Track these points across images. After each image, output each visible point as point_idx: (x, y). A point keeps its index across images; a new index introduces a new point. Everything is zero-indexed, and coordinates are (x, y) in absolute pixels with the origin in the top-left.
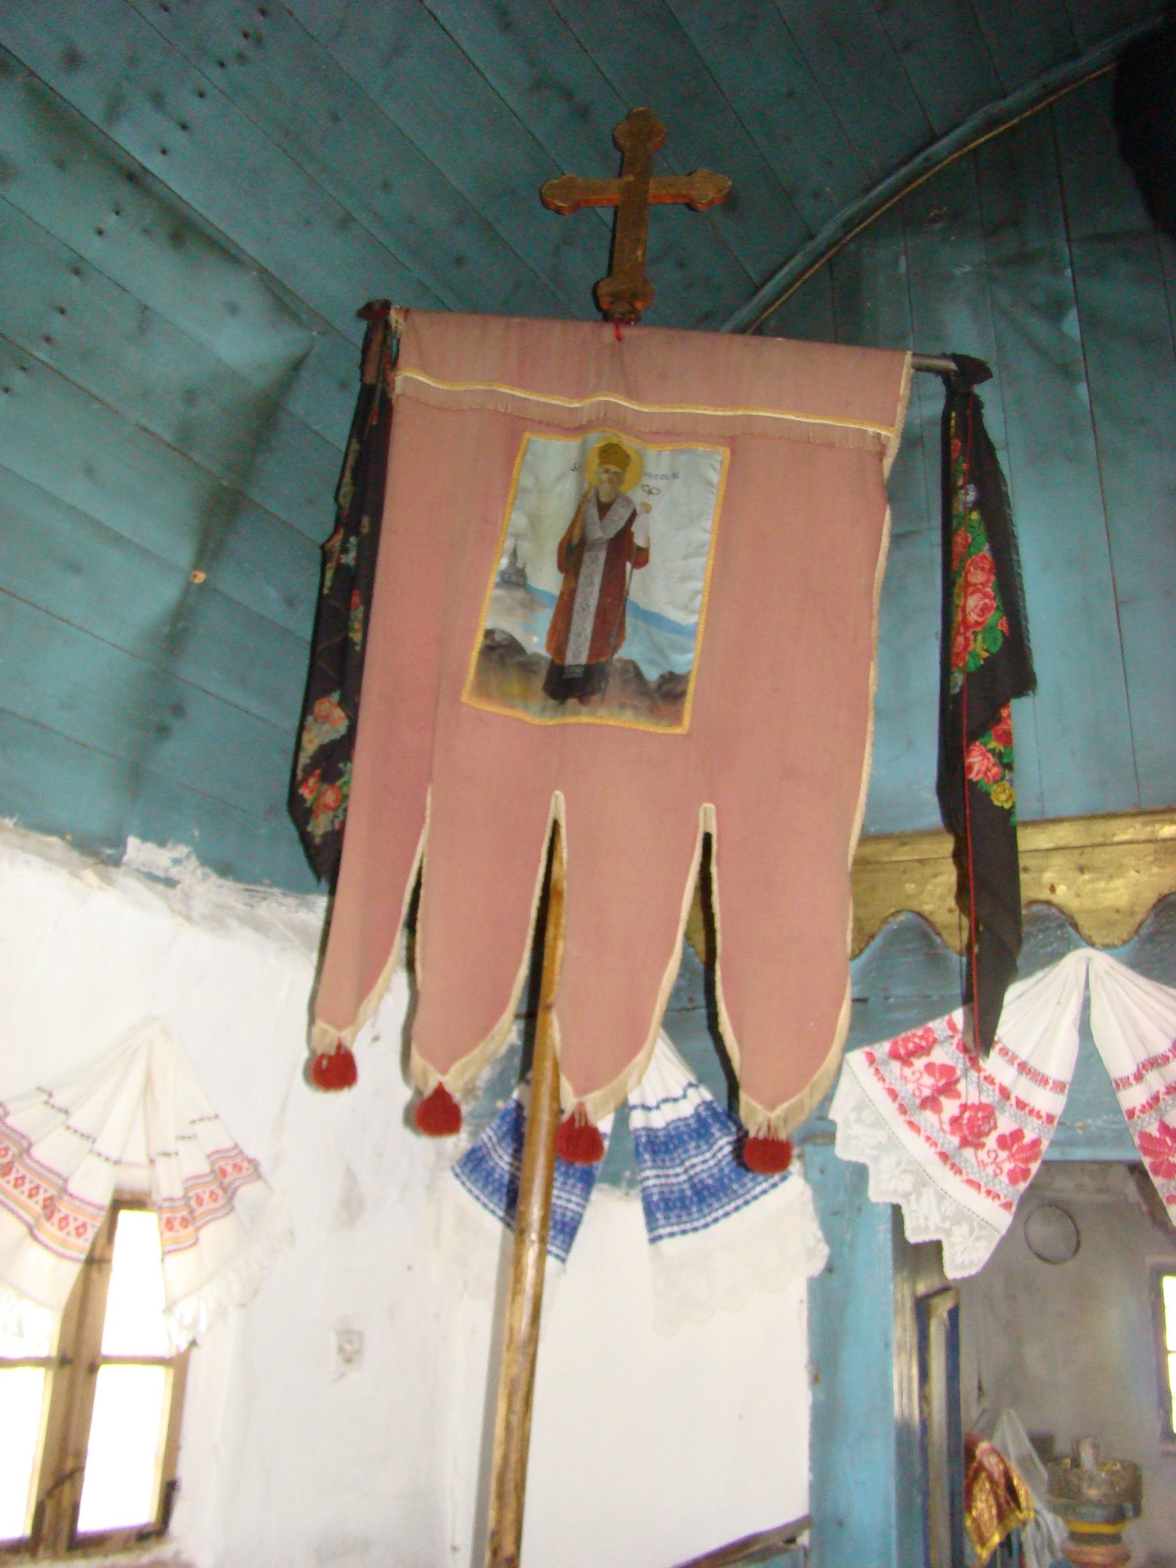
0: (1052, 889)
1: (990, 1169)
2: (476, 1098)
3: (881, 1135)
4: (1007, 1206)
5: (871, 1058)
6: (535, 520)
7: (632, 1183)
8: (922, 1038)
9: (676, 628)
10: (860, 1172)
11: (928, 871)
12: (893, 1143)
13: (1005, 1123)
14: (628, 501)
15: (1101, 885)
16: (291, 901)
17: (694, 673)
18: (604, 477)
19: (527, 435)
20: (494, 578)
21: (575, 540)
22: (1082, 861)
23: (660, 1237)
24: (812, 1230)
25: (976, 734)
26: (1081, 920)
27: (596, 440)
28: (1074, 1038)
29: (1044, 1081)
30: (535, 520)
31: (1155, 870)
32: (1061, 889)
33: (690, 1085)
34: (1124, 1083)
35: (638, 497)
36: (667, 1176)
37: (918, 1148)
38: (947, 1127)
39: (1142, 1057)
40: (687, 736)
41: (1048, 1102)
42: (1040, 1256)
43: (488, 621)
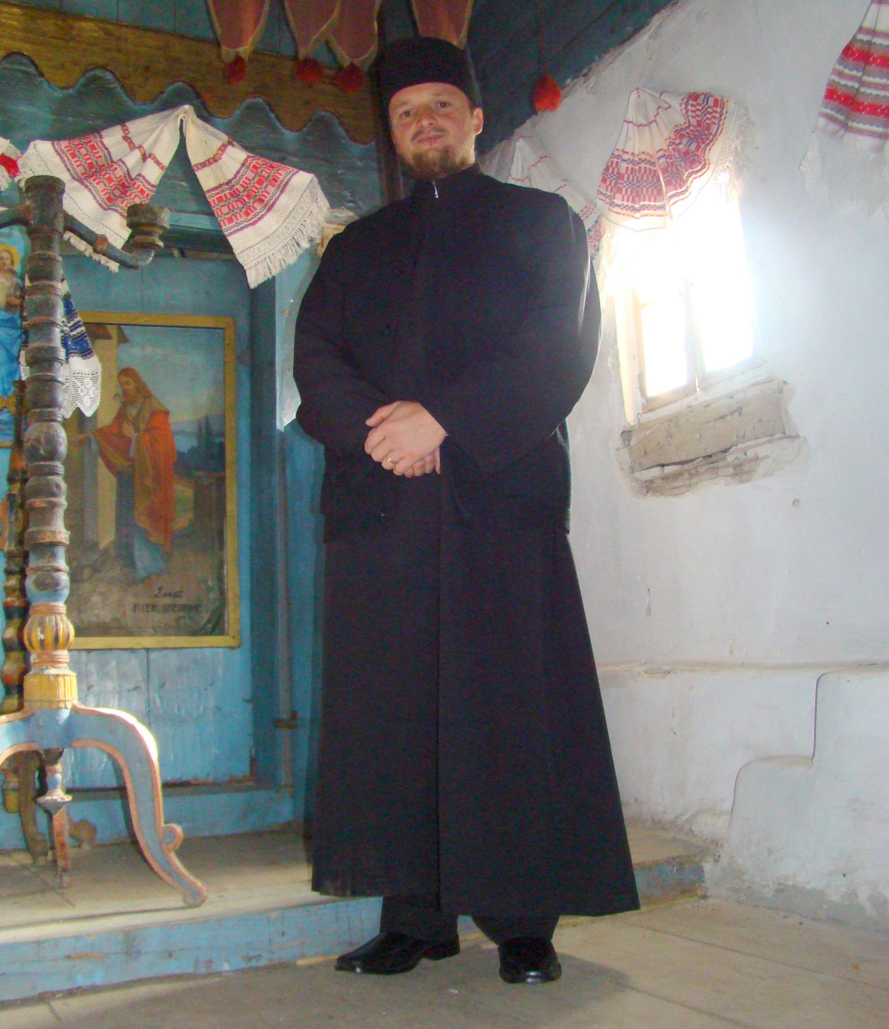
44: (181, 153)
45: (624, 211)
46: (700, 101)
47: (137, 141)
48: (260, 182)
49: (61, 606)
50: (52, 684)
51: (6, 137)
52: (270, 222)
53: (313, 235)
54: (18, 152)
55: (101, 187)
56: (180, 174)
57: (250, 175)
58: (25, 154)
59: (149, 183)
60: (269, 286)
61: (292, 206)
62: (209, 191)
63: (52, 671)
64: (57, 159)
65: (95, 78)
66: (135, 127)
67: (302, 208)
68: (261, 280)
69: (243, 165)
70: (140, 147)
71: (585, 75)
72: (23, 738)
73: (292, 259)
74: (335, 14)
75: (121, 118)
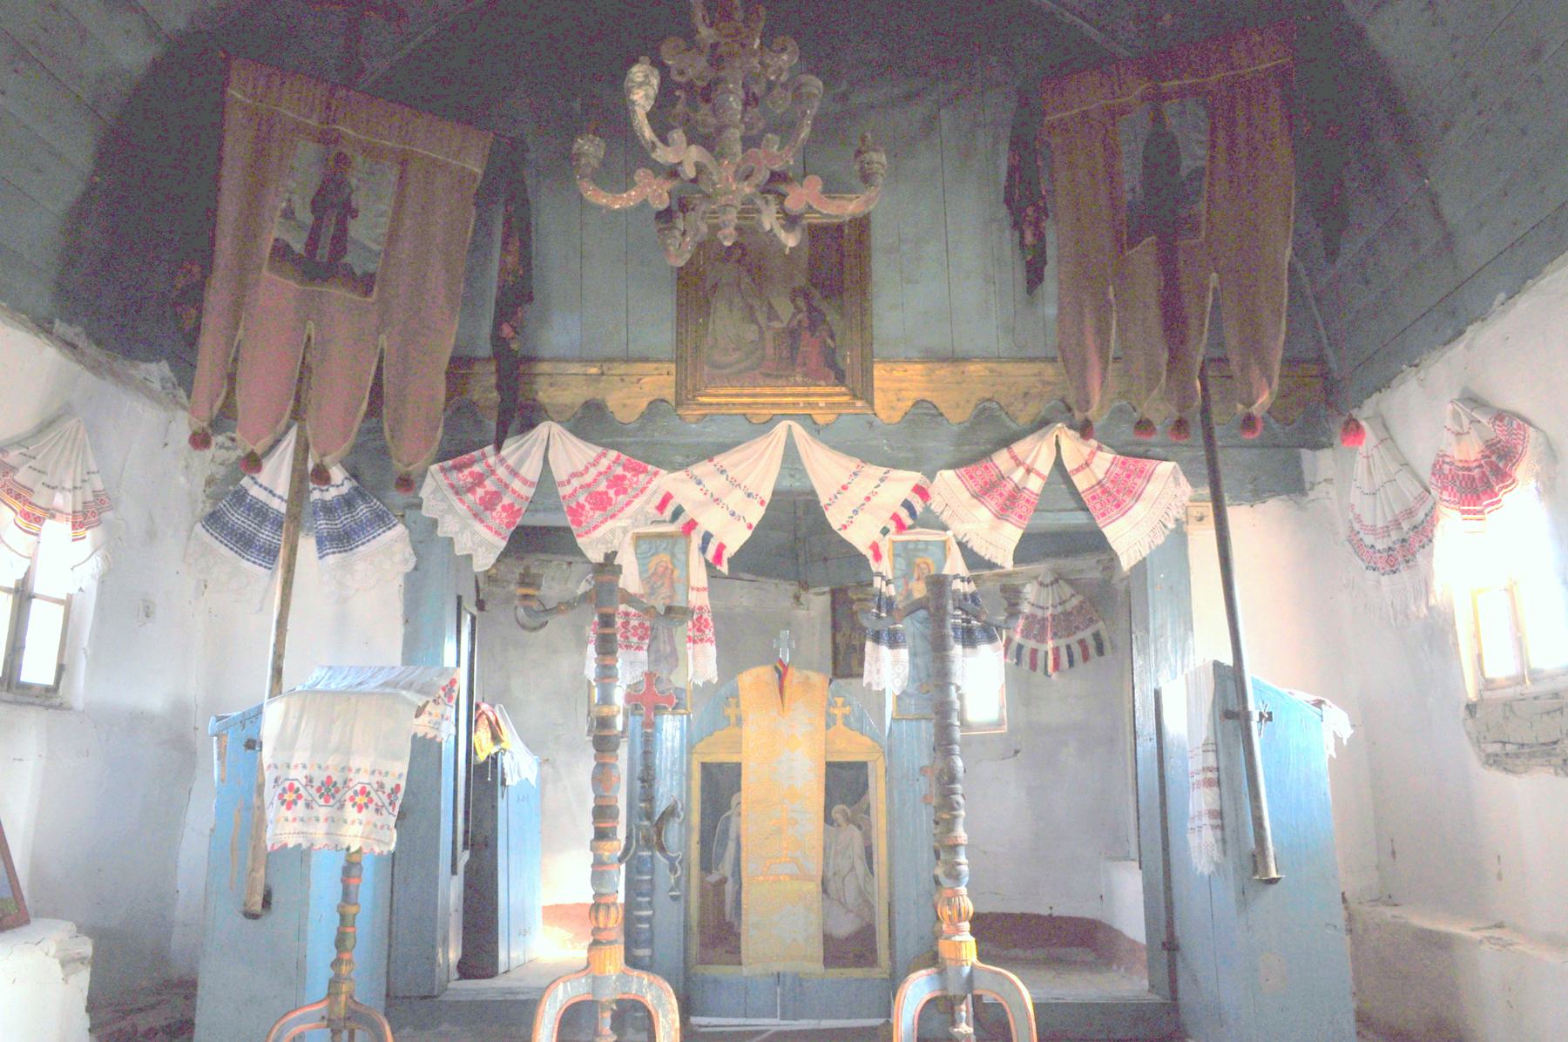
1: (497, 521)
2: (216, 484)
3: (444, 506)
4: (504, 538)
7: (310, 529)
10: (434, 523)
12: (451, 509)
13: (506, 500)
22: (552, 380)
23: (327, 554)
24: (409, 550)
28: (541, 463)
33: (346, 478)
34: (562, 484)
38: (478, 501)
39: (570, 472)
41: (529, 492)
44: (1059, 463)
48: (1128, 476)
51: (918, 471)
52: (1139, 510)
53: (1178, 517)
54: (928, 482)
55: (993, 503)
56: (1060, 479)
57: (1118, 470)
59: (1032, 493)
60: (1141, 567)
64: (959, 482)
65: (985, 409)
66: (1019, 448)
67: (1167, 493)
68: (1133, 563)
69: (1112, 463)
73: (1160, 540)
75: (1006, 442)
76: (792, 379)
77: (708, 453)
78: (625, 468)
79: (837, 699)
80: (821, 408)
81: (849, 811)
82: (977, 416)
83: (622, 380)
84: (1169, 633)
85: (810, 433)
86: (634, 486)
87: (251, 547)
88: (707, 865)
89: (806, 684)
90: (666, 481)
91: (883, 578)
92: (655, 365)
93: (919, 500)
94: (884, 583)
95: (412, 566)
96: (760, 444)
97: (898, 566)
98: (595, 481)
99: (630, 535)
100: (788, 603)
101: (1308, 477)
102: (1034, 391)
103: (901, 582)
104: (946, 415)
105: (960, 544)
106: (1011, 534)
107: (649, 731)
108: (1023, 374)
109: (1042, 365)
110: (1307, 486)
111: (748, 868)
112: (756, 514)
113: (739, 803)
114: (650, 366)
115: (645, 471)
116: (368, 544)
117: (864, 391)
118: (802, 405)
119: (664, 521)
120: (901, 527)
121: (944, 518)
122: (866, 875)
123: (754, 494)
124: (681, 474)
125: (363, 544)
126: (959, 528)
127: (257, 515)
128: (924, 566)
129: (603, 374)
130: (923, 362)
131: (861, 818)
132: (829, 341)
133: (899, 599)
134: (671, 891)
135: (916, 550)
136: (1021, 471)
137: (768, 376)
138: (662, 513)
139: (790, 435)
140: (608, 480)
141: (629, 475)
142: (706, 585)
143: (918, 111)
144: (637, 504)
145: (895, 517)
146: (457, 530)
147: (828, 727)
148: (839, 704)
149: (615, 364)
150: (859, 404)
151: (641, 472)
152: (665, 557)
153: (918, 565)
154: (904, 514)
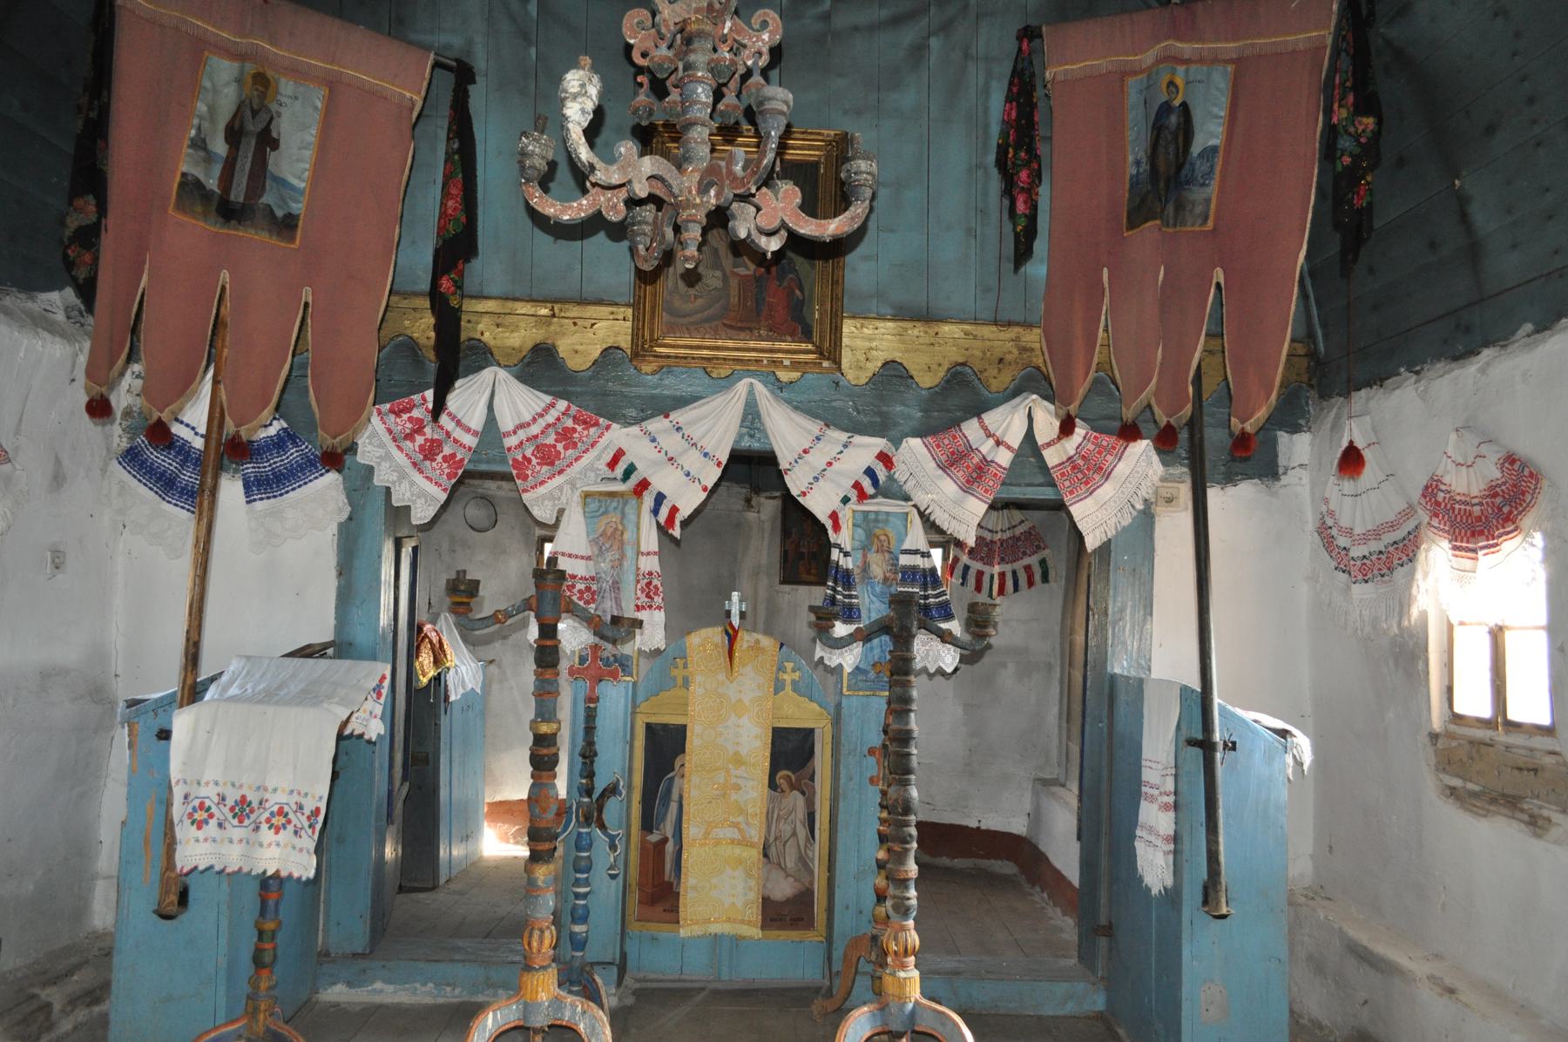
0: (482, 334)
1: (438, 472)
2: (133, 417)
3: (382, 452)
4: (445, 490)
5: (379, 412)
6: (212, 109)
8: (407, 403)
9: (293, 188)
10: (370, 470)
11: (418, 316)
12: (388, 457)
13: (447, 450)
14: (270, 111)
15: (508, 334)
16: (23, 296)
17: (302, 216)
18: (255, 93)
19: (206, 53)
20: (187, 142)
21: (236, 126)
22: (499, 321)
23: (255, 500)
24: (343, 498)
25: (446, 271)
26: (495, 352)
27: (250, 68)
29: (468, 430)
30: (212, 109)
31: (534, 330)
32: (487, 334)
34: (507, 434)
35: (274, 107)
36: (259, 468)
37: (400, 458)
38: (417, 449)
39: (517, 422)
40: (298, 249)
41: (470, 440)
42: (472, 527)
43: (184, 168)
44: (1030, 435)
45: (1441, 533)
46: (1516, 466)
47: (992, 429)
48: (1100, 453)
49: (911, 923)
50: (902, 984)
52: (1107, 491)
53: (1147, 497)
55: (959, 474)
57: (1091, 446)
58: (900, 450)
59: (1001, 467)
60: (1105, 549)
61: (1128, 472)
62: (1053, 468)
63: (902, 974)
64: (925, 450)
66: (990, 418)
67: (1138, 472)
68: (1098, 544)
69: (1085, 438)
70: (994, 435)
71: (1417, 373)
72: (879, 1023)
73: (1127, 521)
74: (1155, 380)
75: (978, 409)
76: (756, 332)
77: (664, 406)
78: (575, 418)
79: (786, 664)
80: (786, 367)
81: (793, 777)
82: (948, 381)
83: (575, 324)
84: (1128, 618)
85: (772, 392)
86: (585, 439)
87: (172, 488)
88: (648, 824)
89: (756, 648)
90: (618, 436)
91: (841, 550)
92: (611, 309)
93: (884, 469)
94: (842, 555)
95: (346, 516)
96: (719, 401)
97: (857, 537)
98: (543, 432)
99: (578, 493)
100: (739, 504)
101: (1282, 461)
102: (1009, 357)
103: (859, 555)
104: (916, 379)
105: (921, 514)
106: (976, 508)
107: (592, 705)
108: (1000, 339)
109: (1020, 330)
110: (1281, 471)
111: (691, 831)
112: (712, 475)
113: (683, 765)
114: (604, 311)
115: (597, 424)
116: (298, 490)
117: (831, 351)
118: (765, 362)
119: (615, 479)
120: (862, 496)
121: (908, 487)
122: (807, 838)
123: (711, 455)
124: (635, 430)
125: (293, 489)
126: (921, 498)
127: (179, 453)
128: (883, 538)
129: (554, 316)
130: (896, 320)
131: (805, 786)
132: (798, 292)
133: (856, 571)
134: (609, 869)
135: (876, 521)
136: (991, 442)
137: (731, 327)
138: (613, 470)
139: (751, 392)
140: (557, 433)
141: (579, 428)
142: (657, 550)
143: (908, 35)
144: (586, 459)
145: (857, 486)
146: (395, 479)
147: (776, 693)
148: (789, 670)
149: (570, 306)
150: (826, 364)
151: (593, 426)
152: (614, 518)
153: (878, 538)
154: (866, 483)
